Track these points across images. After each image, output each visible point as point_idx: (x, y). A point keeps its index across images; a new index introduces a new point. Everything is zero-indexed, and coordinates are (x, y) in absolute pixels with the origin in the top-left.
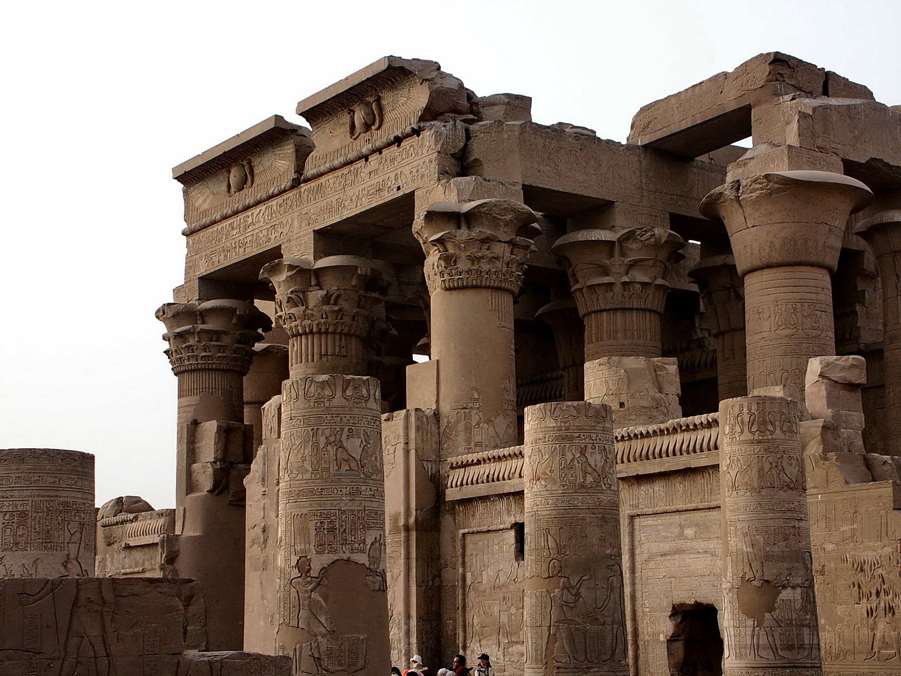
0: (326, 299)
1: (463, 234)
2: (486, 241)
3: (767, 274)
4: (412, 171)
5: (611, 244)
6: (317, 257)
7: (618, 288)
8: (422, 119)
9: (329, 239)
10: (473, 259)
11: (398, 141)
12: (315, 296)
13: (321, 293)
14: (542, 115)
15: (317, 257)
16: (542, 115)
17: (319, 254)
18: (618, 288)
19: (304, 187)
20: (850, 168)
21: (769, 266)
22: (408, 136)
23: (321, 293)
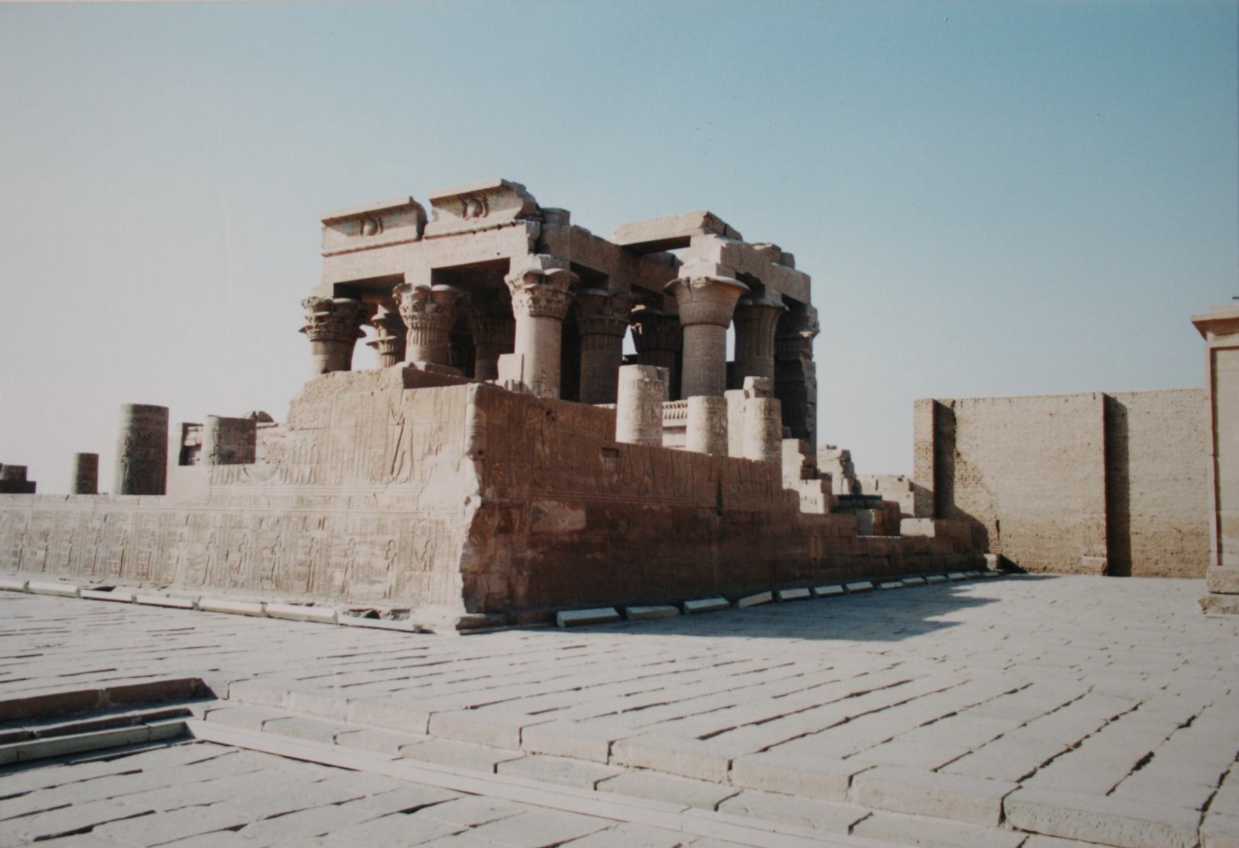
0: (436, 310)
1: (544, 286)
2: (555, 292)
3: (699, 328)
4: (509, 243)
5: (605, 298)
6: (434, 283)
7: (607, 322)
8: (517, 217)
9: (439, 275)
10: (549, 301)
11: (499, 227)
12: (429, 307)
13: (434, 305)
14: (573, 221)
15: (434, 283)
16: (573, 221)
17: (434, 282)
18: (607, 322)
19: (424, 241)
20: (738, 276)
21: (702, 323)
22: (507, 225)
23: (434, 305)
